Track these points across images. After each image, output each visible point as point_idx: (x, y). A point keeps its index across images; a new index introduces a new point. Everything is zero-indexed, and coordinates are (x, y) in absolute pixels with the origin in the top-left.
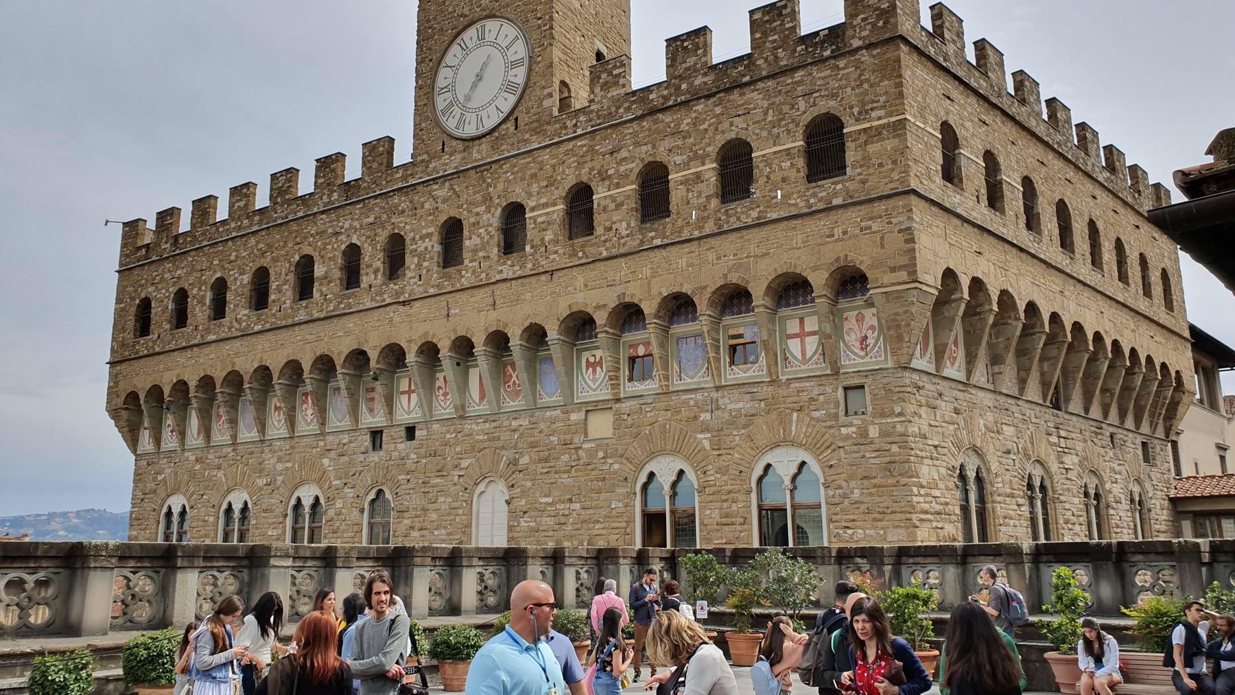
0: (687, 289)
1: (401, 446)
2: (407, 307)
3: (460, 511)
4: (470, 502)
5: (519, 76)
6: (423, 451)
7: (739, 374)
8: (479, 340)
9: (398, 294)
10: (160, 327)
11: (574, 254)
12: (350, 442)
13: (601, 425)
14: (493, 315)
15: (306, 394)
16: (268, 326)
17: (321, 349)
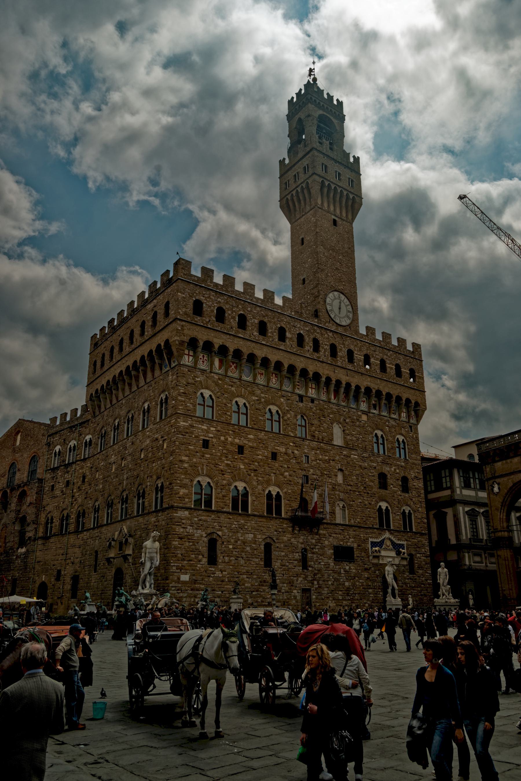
0: (391, 392)
1: (311, 404)
5: (351, 315)
6: (318, 408)
7: (393, 416)
8: (344, 383)
9: (319, 357)
10: (210, 317)
13: (364, 418)
14: (347, 378)
15: (273, 374)
16: (268, 344)
17: (291, 362)
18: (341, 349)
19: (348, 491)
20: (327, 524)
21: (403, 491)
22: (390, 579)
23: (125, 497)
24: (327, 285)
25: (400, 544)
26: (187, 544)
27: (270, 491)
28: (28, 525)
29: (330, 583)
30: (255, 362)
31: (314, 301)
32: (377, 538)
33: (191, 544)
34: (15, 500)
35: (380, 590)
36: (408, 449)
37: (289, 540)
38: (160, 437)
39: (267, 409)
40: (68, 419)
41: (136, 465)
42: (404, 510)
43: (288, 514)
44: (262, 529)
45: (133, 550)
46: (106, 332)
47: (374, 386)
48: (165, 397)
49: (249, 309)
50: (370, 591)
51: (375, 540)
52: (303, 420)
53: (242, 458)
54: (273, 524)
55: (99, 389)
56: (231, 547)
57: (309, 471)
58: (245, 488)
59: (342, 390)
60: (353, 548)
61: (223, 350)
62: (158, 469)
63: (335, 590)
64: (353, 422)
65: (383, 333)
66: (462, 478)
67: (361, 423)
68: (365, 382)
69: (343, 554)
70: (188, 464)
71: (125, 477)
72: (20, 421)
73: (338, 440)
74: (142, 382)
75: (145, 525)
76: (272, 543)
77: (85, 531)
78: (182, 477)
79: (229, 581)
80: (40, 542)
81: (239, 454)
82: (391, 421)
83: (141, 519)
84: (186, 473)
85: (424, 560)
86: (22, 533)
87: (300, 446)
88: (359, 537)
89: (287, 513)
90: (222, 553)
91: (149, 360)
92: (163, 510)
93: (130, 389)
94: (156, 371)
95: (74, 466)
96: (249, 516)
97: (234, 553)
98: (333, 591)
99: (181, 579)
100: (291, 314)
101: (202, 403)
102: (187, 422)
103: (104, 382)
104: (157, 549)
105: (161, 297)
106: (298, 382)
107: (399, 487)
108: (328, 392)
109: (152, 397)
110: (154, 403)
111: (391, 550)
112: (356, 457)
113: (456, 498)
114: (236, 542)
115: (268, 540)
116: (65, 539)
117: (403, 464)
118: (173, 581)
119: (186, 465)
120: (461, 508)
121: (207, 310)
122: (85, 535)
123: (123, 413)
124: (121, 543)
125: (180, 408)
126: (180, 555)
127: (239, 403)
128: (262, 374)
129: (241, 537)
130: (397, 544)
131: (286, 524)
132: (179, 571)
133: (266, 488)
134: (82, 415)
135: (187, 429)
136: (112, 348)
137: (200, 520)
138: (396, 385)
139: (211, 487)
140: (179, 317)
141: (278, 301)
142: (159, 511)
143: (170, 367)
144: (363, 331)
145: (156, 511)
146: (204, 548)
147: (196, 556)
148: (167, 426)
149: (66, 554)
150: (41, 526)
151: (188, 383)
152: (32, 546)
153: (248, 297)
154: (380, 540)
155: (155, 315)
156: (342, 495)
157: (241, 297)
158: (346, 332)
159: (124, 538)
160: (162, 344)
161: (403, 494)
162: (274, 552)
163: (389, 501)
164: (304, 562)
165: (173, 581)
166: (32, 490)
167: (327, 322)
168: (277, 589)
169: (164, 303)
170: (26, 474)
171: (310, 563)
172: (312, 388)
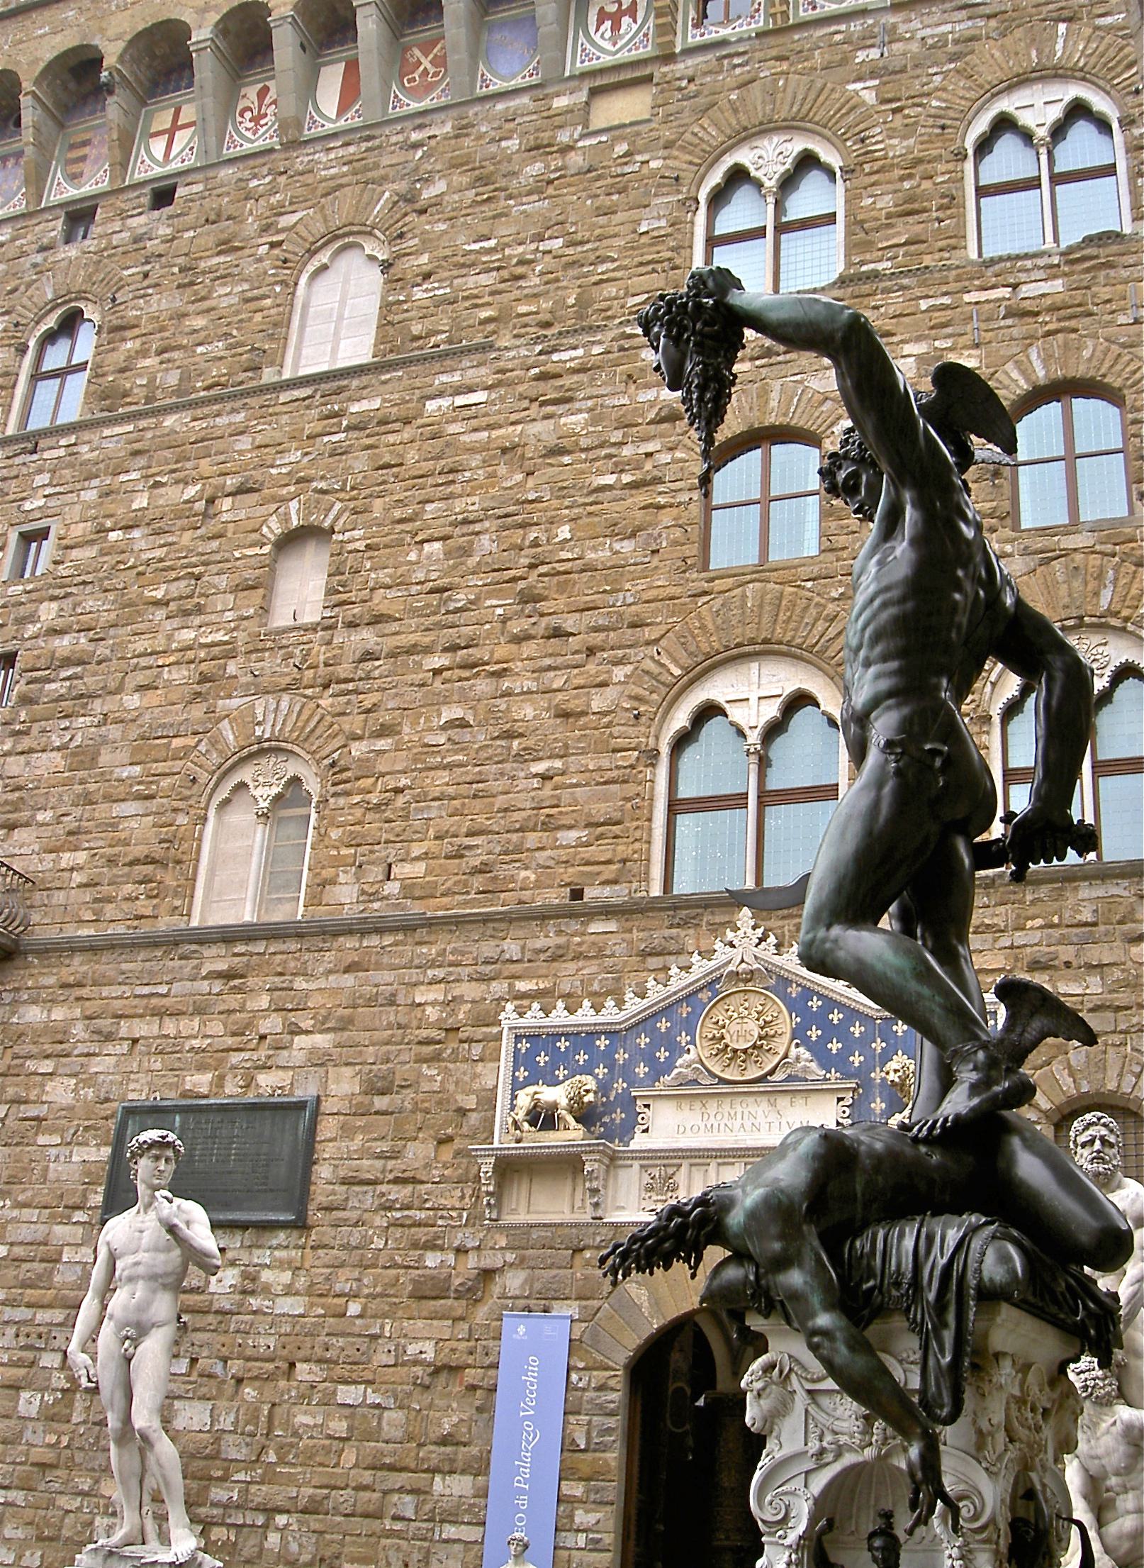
3: (268, 302)
4: (290, 286)
12: (13, 240)
20: (92, 948)
51: (585, 1016)
60: (301, 1106)
63: (71, 1466)
88: (390, 1015)
98: (43, 1466)
112: (480, 396)
117: (1057, 285)
154: (634, 1006)
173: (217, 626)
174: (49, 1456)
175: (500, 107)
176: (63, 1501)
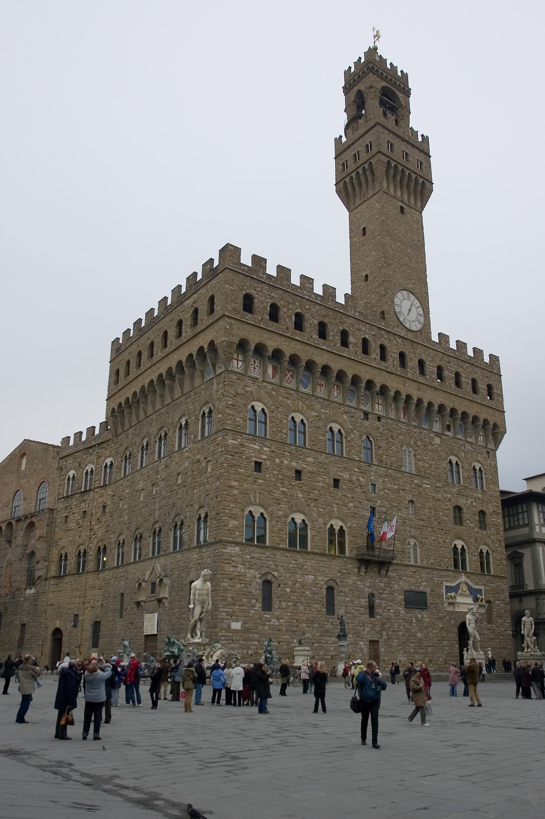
0: (468, 412)
1: (377, 423)
2: (389, 375)
5: (422, 320)
9: (386, 367)
10: (263, 314)
11: (441, 387)
13: (437, 440)
14: (419, 393)
17: (356, 372)
18: (411, 359)
19: (420, 527)
20: (397, 564)
21: (481, 528)
22: (471, 628)
23: (157, 530)
24: (394, 283)
25: (477, 590)
26: (238, 586)
27: (332, 525)
28: (38, 563)
29: (400, 633)
30: (314, 371)
31: (380, 300)
32: (452, 582)
33: (243, 585)
34: (22, 533)
35: (455, 642)
36: (486, 478)
37: (353, 583)
38: (202, 458)
39: (328, 428)
40: (84, 438)
41: (172, 491)
42: (481, 550)
43: (353, 552)
44: (324, 569)
45: (170, 592)
46: (131, 335)
47: (449, 403)
48: (207, 411)
49: (307, 307)
50: (445, 643)
52: (369, 442)
53: (300, 485)
54: (337, 565)
55: (123, 403)
56: (288, 590)
57: (376, 502)
58: (303, 520)
59: (413, 407)
60: (425, 593)
61: (277, 355)
62: (200, 496)
64: (425, 446)
65: (457, 342)
66: (541, 514)
67: (434, 447)
68: (438, 399)
69: (416, 600)
70: (238, 490)
71: (157, 506)
72: (25, 442)
73: (410, 465)
74: (177, 393)
75: (185, 562)
76: (335, 586)
77: (108, 569)
78: (232, 505)
79: (287, 630)
80: (52, 582)
81: (296, 480)
82: (467, 445)
83: (179, 556)
84: (235, 502)
85: (504, 607)
86: (30, 572)
87: (366, 473)
88: (432, 581)
89: (352, 551)
90: (278, 597)
91: (187, 367)
92: (207, 544)
93: (163, 402)
94: (196, 380)
95: (91, 493)
96: (309, 553)
97: (292, 597)
99: (232, 628)
100: (355, 315)
101: (253, 418)
102: (236, 440)
103: (130, 394)
104: (208, 590)
105: (203, 291)
106: (363, 396)
107: (476, 523)
108: (397, 410)
109: (191, 411)
110: (193, 418)
111: (467, 596)
112: (429, 486)
113: (536, 536)
114: (295, 584)
115: (331, 584)
116: (83, 578)
117: (481, 496)
118: (222, 629)
119: (236, 492)
120: (540, 549)
121: (259, 307)
122: (107, 574)
123: (154, 430)
124: (153, 584)
125: (229, 422)
126: (230, 599)
127: (296, 419)
128: (322, 385)
129: (300, 578)
130: (475, 589)
131: (351, 564)
132: (229, 617)
133: (328, 521)
134: (100, 433)
135: (236, 448)
136: (140, 354)
137: (253, 558)
138: (473, 403)
139: (265, 519)
140: (226, 314)
141: (340, 299)
142: (203, 546)
143: (215, 373)
144: (435, 338)
145: (199, 546)
146: (259, 591)
147: (249, 600)
148: (211, 445)
149: (85, 597)
150: (53, 564)
151: (238, 394)
152: (42, 587)
153: (306, 293)
154: (456, 584)
155: (196, 311)
156: (413, 532)
157: (298, 292)
158: (416, 338)
159: (158, 578)
160: (206, 347)
161: (481, 531)
162: (338, 597)
163: (466, 538)
164: (371, 610)
165: (222, 629)
166: (42, 522)
167: (395, 326)
168: (346, 640)
169: (208, 298)
170: (33, 504)
171: (378, 610)
172: (378, 404)
173: (404, 514)
174: (403, 641)
175: (424, 431)
176: (407, 647)
